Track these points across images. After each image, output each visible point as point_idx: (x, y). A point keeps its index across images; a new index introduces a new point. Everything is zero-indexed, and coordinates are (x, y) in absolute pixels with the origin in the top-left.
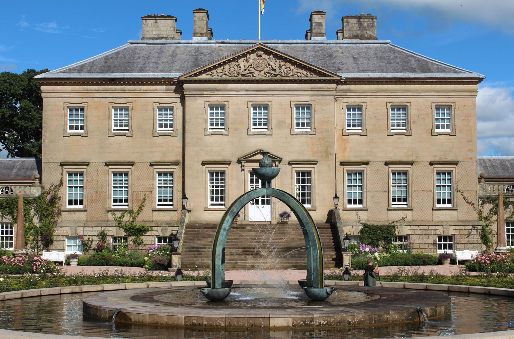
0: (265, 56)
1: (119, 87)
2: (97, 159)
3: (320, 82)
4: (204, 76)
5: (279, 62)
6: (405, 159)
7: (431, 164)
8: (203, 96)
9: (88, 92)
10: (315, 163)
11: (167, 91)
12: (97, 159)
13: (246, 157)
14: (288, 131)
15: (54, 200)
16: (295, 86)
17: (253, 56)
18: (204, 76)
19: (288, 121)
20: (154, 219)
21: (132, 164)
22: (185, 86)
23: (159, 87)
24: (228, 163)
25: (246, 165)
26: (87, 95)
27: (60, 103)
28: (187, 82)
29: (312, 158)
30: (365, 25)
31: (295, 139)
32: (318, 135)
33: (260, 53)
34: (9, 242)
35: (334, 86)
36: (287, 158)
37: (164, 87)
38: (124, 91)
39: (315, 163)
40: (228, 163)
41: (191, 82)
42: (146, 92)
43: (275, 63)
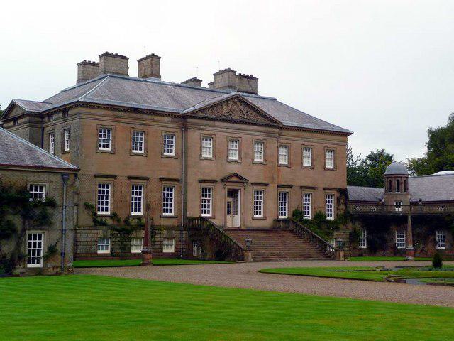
0: (239, 104)
1: (139, 115)
2: (122, 174)
3: (271, 126)
4: (200, 114)
5: (246, 108)
6: (310, 185)
7: (324, 189)
8: (199, 129)
10: (266, 185)
11: (172, 122)
12: (122, 174)
14: (249, 161)
16: (256, 128)
20: (162, 224)
21: (147, 179)
22: (189, 120)
23: (166, 119)
25: (227, 184)
26: (115, 118)
27: (94, 123)
28: (191, 117)
29: (264, 182)
31: (255, 167)
33: (236, 101)
34: (37, 241)
35: (277, 130)
36: (251, 180)
38: (140, 119)
39: (266, 185)
40: (214, 182)
41: (193, 117)
43: (245, 110)
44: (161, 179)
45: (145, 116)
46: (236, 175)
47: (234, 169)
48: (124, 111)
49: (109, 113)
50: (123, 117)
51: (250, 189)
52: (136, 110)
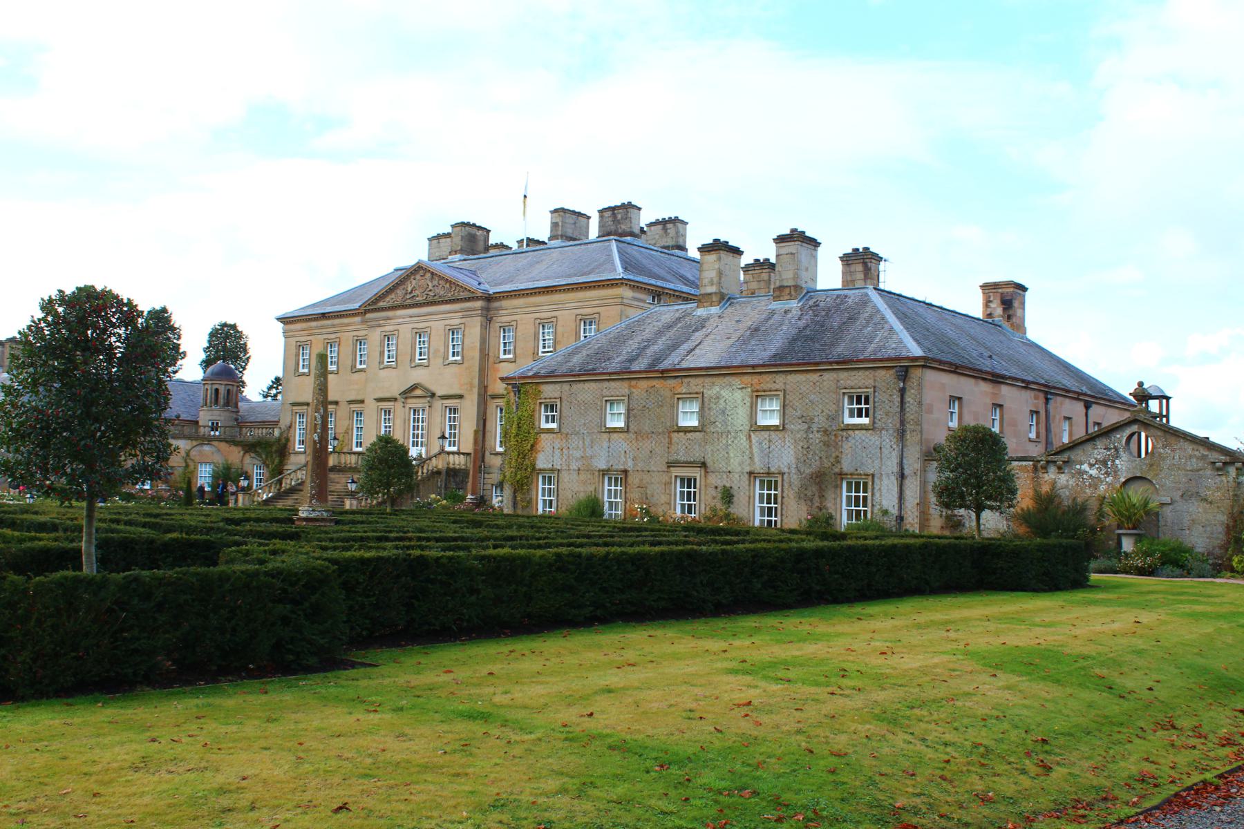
4: (381, 304)
8: (379, 326)
9: (311, 329)
10: (461, 397)
13: (404, 392)
15: (288, 440)
17: (418, 277)
18: (381, 304)
19: (442, 349)
22: (369, 316)
24: (395, 400)
30: (619, 217)
32: (466, 365)
33: (422, 272)
36: (439, 393)
37: (358, 319)
38: (334, 326)
39: (461, 397)
40: (395, 400)
42: (348, 325)
44: (350, 402)
45: (337, 321)
46: (414, 387)
47: (418, 376)
48: (315, 320)
49: (304, 325)
50: (317, 328)
51: (438, 404)
52: (324, 316)
